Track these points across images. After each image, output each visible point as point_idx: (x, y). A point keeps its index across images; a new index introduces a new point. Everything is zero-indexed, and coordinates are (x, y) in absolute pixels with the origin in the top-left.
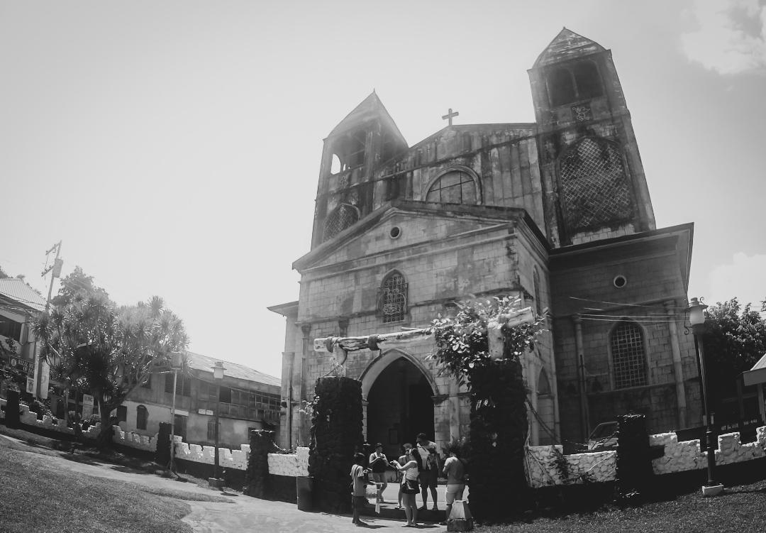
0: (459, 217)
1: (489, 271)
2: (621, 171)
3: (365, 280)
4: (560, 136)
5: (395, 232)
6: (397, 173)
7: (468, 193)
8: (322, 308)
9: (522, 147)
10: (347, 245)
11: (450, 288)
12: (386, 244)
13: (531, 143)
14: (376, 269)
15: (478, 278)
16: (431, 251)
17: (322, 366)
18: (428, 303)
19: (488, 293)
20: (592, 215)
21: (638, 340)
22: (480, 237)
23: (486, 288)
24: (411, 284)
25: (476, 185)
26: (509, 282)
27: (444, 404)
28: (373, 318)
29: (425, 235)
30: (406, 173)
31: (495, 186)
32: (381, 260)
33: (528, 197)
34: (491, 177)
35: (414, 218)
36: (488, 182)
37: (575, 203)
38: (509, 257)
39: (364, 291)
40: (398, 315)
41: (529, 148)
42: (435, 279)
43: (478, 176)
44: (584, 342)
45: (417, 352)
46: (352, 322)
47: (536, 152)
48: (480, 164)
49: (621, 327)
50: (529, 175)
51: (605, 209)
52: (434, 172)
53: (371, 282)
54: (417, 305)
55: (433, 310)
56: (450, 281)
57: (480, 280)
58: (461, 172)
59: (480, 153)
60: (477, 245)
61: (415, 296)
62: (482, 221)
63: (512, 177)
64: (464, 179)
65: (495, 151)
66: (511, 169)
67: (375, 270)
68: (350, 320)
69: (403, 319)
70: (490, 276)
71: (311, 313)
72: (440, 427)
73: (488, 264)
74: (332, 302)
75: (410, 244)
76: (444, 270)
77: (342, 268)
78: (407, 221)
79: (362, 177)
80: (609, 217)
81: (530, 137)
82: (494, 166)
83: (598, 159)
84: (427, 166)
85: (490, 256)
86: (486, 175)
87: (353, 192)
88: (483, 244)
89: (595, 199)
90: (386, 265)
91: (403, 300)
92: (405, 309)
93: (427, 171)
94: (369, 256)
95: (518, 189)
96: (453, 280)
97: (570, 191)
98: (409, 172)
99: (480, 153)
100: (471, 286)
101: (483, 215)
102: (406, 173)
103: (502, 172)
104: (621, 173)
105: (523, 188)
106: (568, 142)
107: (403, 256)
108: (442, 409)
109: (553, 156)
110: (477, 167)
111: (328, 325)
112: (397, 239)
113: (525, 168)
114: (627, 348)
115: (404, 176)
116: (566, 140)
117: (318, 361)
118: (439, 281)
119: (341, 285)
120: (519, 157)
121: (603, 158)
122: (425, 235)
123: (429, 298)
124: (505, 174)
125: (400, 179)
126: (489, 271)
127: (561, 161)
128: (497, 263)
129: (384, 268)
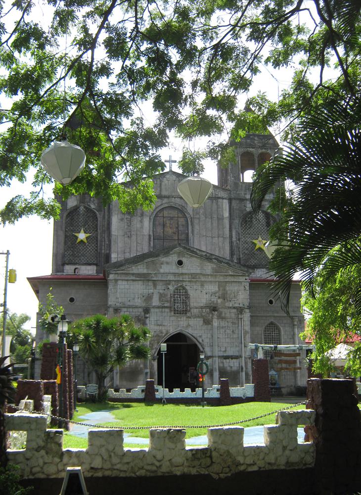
3: (160, 288)
5: (180, 263)
7: (183, 225)
14: (168, 282)
16: (203, 279)
18: (202, 308)
22: (230, 277)
28: (167, 310)
32: (171, 278)
33: (221, 239)
34: (199, 219)
42: (205, 295)
46: (152, 310)
55: (204, 311)
61: (193, 303)
63: (212, 223)
64: (180, 215)
67: (168, 283)
69: (186, 313)
78: (187, 257)
81: (225, 199)
82: (201, 212)
86: (196, 217)
88: (232, 282)
90: (175, 281)
91: (186, 303)
92: (189, 309)
97: (245, 242)
103: (206, 218)
105: (218, 232)
113: (220, 219)
121: (266, 226)
124: (207, 219)
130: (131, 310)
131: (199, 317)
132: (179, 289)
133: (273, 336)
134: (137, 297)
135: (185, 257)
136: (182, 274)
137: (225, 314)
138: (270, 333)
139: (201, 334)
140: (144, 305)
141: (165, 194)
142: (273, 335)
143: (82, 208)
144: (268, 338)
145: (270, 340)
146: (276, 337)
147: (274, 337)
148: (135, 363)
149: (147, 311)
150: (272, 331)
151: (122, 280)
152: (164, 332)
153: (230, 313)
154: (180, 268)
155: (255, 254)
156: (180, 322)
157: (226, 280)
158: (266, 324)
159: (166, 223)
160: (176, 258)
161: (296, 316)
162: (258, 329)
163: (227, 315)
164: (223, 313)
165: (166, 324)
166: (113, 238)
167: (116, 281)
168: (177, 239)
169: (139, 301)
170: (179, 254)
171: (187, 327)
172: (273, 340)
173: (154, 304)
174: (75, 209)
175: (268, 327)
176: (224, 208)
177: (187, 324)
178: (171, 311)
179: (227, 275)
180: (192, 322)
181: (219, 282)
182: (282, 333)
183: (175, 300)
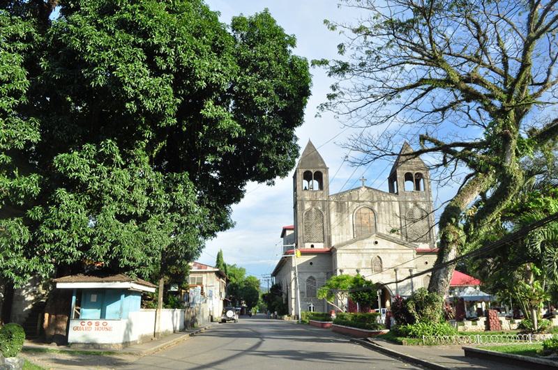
32: (371, 251)
46: (361, 270)
65: (383, 203)
140: (357, 267)
143: (313, 209)
166: (332, 227)
174: (309, 211)
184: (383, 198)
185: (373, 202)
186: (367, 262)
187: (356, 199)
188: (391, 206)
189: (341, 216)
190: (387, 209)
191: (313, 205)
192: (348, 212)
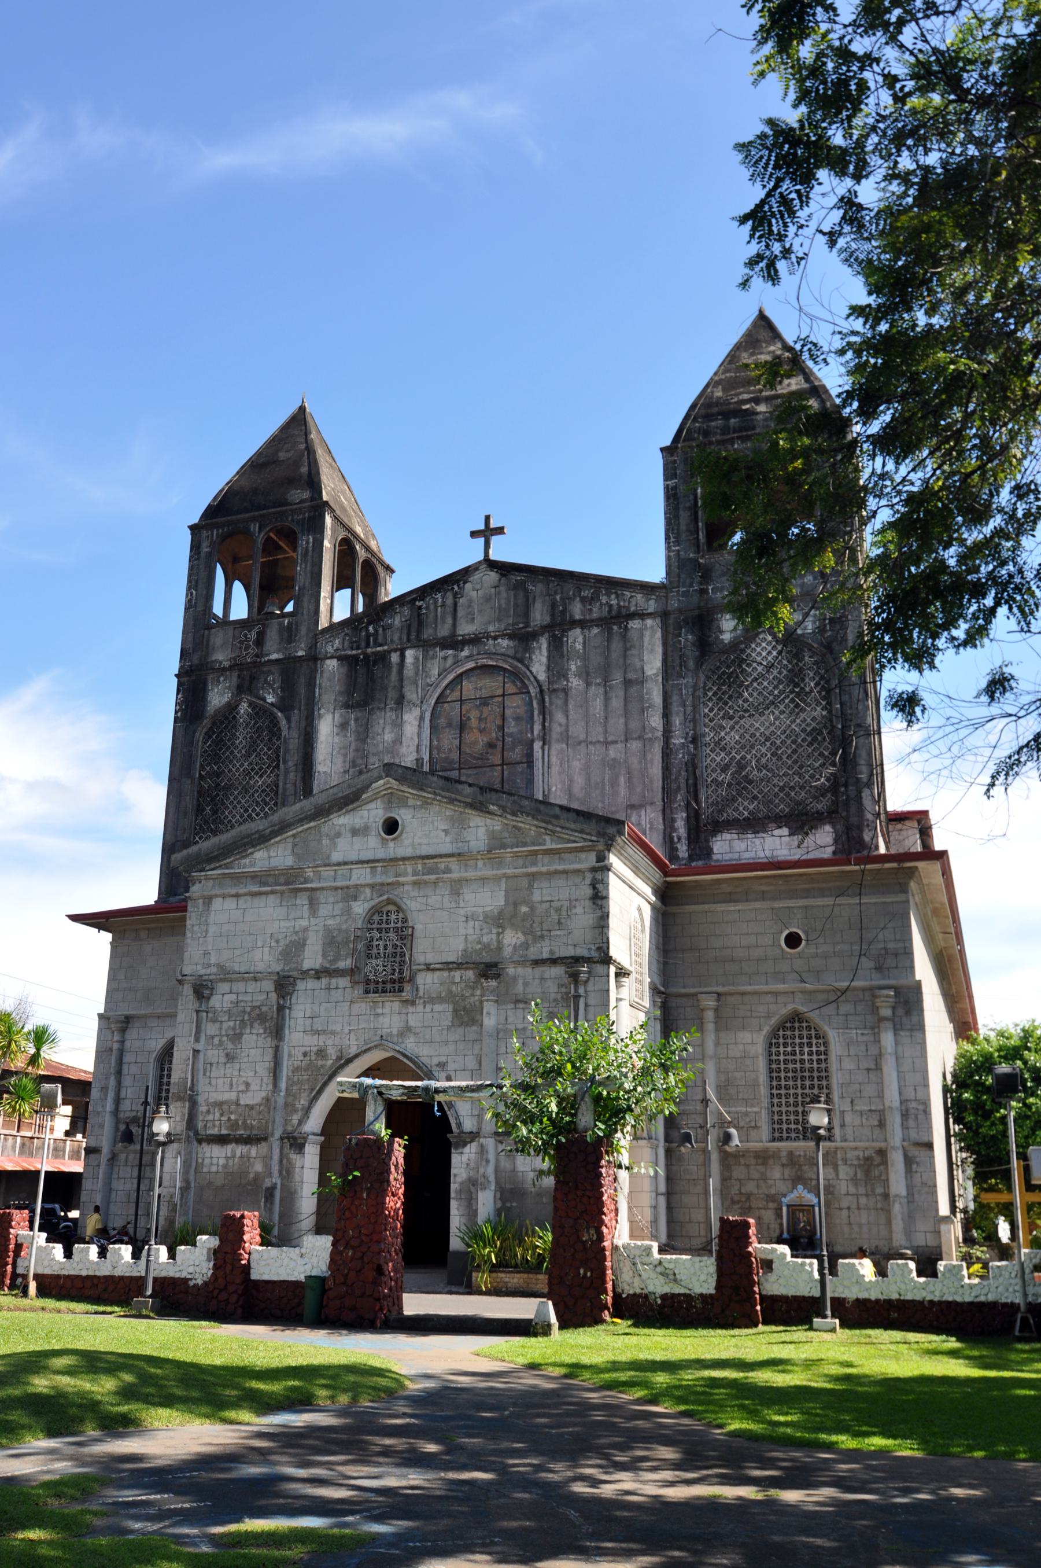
0: (509, 816)
1: (559, 923)
2: (824, 713)
3: (330, 911)
4: (712, 621)
5: (391, 827)
6: (369, 650)
7: (518, 719)
8: (238, 952)
9: (633, 635)
10: (294, 836)
11: (489, 945)
12: (373, 846)
13: (652, 627)
14: (352, 891)
15: (539, 933)
17: (237, 1066)
18: (448, 966)
19: (554, 961)
20: (755, 798)
21: (818, 1053)
22: (546, 859)
23: (551, 952)
24: (419, 927)
25: (535, 704)
26: (592, 946)
27: (470, 1151)
28: (344, 982)
29: (448, 840)
30: (389, 652)
31: (571, 712)
32: (361, 876)
33: (635, 745)
34: (566, 691)
35: (428, 804)
36: (560, 702)
37: (725, 769)
38: (594, 903)
39: (327, 930)
40: (393, 981)
41: (646, 639)
43: (540, 686)
44: (717, 1044)
45: (425, 1053)
46: (301, 985)
47: (659, 650)
48: (544, 660)
49: (788, 1025)
50: (641, 699)
51: (782, 789)
52: (450, 661)
53: (342, 914)
54: (428, 968)
55: (457, 980)
56: (491, 932)
57: (542, 937)
58: (505, 669)
59: (547, 635)
60: (540, 874)
61: (423, 951)
62: (551, 831)
63: (607, 699)
64: (510, 688)
66: (606, 680)
67: (351, 893)
68: (298, 982)
69: (401, 990)
70: (558, 933)
71: (213, 961)
72: (460, 1192)
73: (558, 910)
74: (259, 944)
75: (418, 853)
76: (480, 910)
77: (282, 880)
78: (414, 807)
79: (290, 641)
80: (788, 805)
81: (650, 615)
82: (573, 668)
83: (780, 682)
84: (434, 645)
85: (561, 897)
86: (556, 686)
87: (269, 673)
89: (765, 767)
90: (372, 886)
91: (403, 955)
92: (406, 974)
93: (434, 657)
94: (339, 864)
95: (617, 724)
96: (495, 931)
97: (717, 743)
98: (395, 650)
99: (547, 635)
100: (525, 946)
101: (555, 822)
102: (389, 652)
103: (588, 684)
104: (823, 717)
105: (626, 724)
106: (726, 637)
107: (406, 874)
108: (465, 1158)
109: (691, 664)
110: (539, 665)
111: (252, 987)
112: (394, 839)
113: (633, 683)
114: (798, 1065)
115: (383, 657)
116: (721, 632)
117: (227, 1055)
118: (471, 930)
119: (282, 912)
120: (625, 657)
122: (448, 840)
123: (452, 958)
125: (375, 663)
126: (559, 923)
127: (708, 678)
128: (574, 911)
129: (368, 891)
130: (240, 987)
131: (440, 999)
132: (385, 910)
133: (802, 1061)
134: (259, 944)
135: (406, 806)
136: (394, 860)
137: (526, 984)
138: (794, 1053)
139: (443, 1059)
140: (277, 967)
141: (466, 632)
142: (806, 1057)
143: (244, 708)
144: (786, 1070)
145: (795, 1078)
146: (815, 1065)
147: (807, 1065)
148: (242, 1157)
149: (284, 985)
150: (801, 1045)
151: (224, 897)
152: (332, 1053)
153: (542, 979)
154: (391, 844)
155: (750, 782)
156: (381, 1018)
157: (534, 869)
158: (774, 1021)
159: (469, 719)
160: (380, 812)
161: (889, 987)
162: (746, 1036)
163: (529, 990)
164: (521, 982)
165: (338, 1028)
167: (209, 900)
168: (499, 762)
169: (266, 958)
170: (391, 799)
171: (401, 1034)
172: (803, 1078)
173: (307, 965)
175: (784, 1028)
176: (646, 644)
177: (402, 1024)
178: (354, 983)
179: (535, 853)
180: (416, 1017)
181: (508, 877)
182: (836, 1048)
183: (369, 947)
184: (577, 610)
185: (524, 638)
186: (331, 941)
187: (444, 631)
188: (616, 645)
189: (364, 735)
190: (596, 660)
191: (241, 689)
192: (400, 702)
